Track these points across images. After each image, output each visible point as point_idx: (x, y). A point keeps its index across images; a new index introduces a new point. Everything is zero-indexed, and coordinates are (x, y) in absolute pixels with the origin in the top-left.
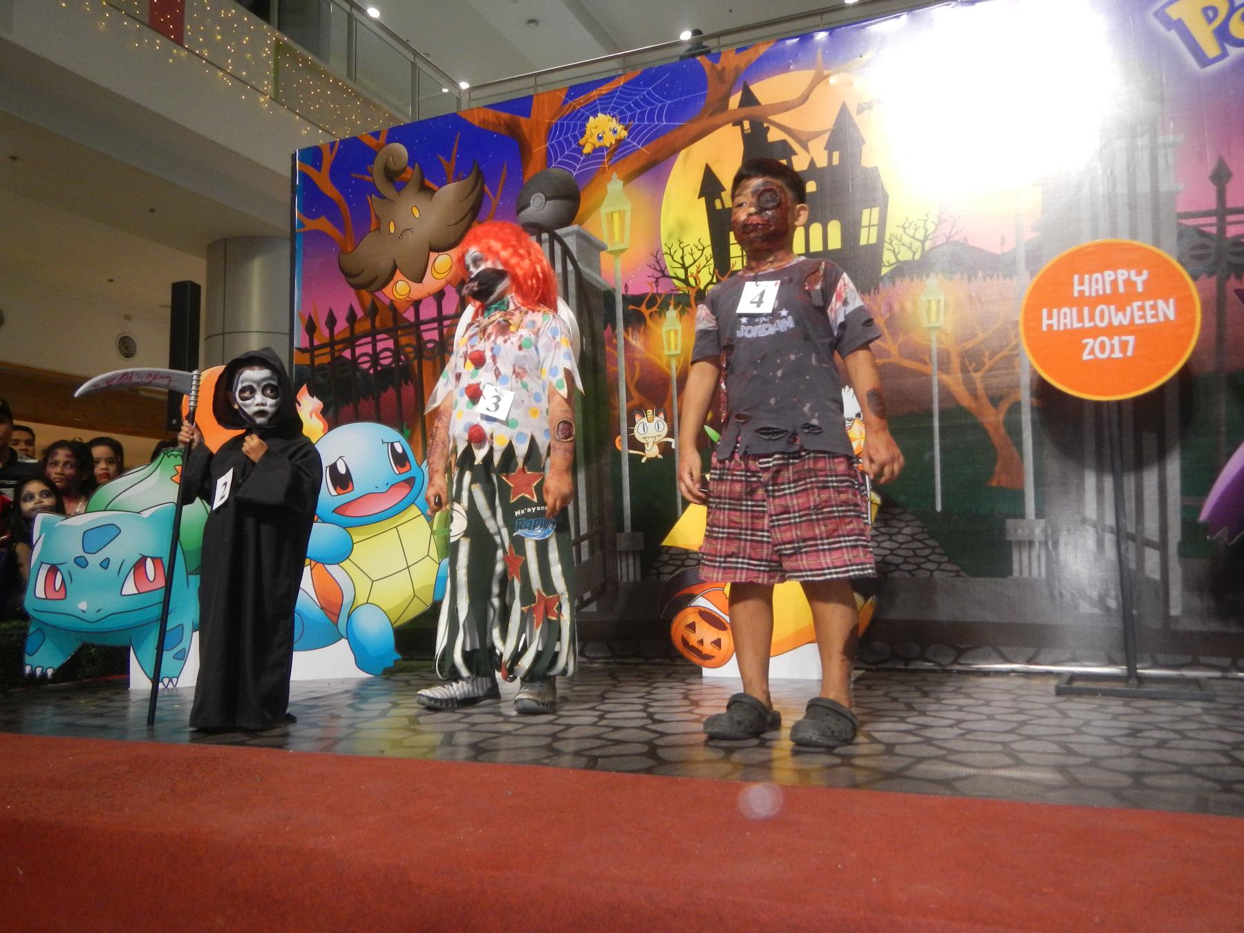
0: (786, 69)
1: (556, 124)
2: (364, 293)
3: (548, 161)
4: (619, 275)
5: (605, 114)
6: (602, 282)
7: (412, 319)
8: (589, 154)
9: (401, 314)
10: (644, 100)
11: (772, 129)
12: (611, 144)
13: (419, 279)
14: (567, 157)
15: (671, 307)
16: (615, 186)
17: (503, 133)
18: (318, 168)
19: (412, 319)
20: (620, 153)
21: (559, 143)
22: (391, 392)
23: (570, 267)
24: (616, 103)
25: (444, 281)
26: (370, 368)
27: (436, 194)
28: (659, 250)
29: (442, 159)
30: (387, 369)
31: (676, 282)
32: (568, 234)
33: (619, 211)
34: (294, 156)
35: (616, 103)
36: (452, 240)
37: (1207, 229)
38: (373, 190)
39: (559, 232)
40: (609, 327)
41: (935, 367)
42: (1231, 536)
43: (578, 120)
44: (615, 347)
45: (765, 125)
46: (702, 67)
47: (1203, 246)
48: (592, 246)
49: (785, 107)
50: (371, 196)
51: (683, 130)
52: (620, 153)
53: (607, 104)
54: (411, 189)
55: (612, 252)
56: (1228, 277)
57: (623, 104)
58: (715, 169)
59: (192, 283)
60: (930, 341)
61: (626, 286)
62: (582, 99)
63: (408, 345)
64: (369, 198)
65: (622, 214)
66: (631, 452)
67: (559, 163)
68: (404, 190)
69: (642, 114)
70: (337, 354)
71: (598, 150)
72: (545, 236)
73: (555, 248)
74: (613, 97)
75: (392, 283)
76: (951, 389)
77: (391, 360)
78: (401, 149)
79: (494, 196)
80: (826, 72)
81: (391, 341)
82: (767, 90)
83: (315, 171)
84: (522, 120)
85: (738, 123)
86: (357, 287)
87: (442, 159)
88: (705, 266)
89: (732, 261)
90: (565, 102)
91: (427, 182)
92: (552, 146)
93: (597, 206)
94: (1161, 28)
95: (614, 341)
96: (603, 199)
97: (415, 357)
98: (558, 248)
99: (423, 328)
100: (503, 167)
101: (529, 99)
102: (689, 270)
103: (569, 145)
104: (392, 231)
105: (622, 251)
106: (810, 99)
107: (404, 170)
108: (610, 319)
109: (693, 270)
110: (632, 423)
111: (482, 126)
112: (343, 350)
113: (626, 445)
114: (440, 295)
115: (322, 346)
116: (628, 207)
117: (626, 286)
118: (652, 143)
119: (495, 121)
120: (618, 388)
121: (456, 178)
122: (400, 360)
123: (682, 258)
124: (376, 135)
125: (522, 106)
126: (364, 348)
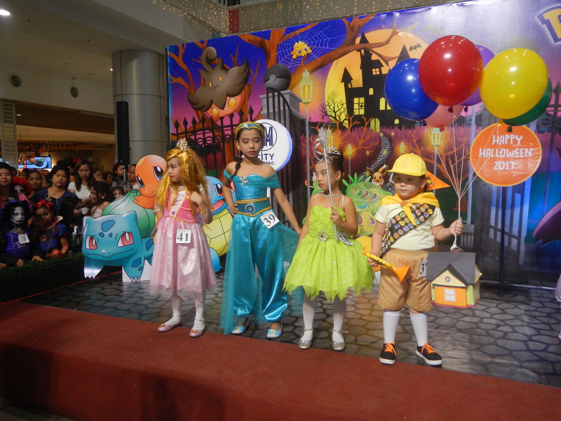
0: (381, 28)
1: (281, 44)
2: (199, 112)
3: (277, 60)
4: (307, 113)
5: (302, 41)
6: (300, 116)
7: (220, 125)
8: (295, 59)
9: (215, 123)
10: (319, 36)
11: (373, 54)
12: (304, 55)
13: (223, 108)
14: (285, 59)
15: (329, 128)
16: (306, 74)
17: (258, 46)
18: (177, 55)
19: (220, 125)
20: (308, 60)
21: (282, 53)
22: (212, 155)
23: (287, 108)
24: (307, 37)
25: (233, 109)
26: (202, 144)
27: (229, 71)
28: (324, 104)
29: (232, 56)
30: (210, 145)
31: (331, 117)
32: (286, 94)
33: (308, 85)
34: (166, 49)
35: (307, 37)
36: (237, 92)
37: (550, 112)
38: (201, 66)
39: (282, 92)
40: (303, 134)
41: (436, 161)
42: (544, 243)
43: (290, 43)
44: (305, 143)
45: (371, 52)
46: (344, 24)
47: (547, 120)
48: (296, 100)
49: (380, 45)
50: (201, 70)
51: (335, 51)
52: (308, 60)
53: (303, 37)
54: (218, 69)
55: (304, 103)
56: (556, 133)
57: (310, 38)
58: (348, 70)
59: (125, 102)
60: (434, 150)
61: (310, 118)
62: (292, 34)
63: (218, 136)
64: (200, 71)
65: (309, 87)
66: (311, 187)
67: (283, 62)
68: (215, 68)
69: (318, 43)
70: (188, 137)
71: (299, 57)
72: (276, 94)
73: (281, 99)
74: (306, 34)
75: (211, 108)
76: (442, 171)
77: (211, 141)
78: (213, 49)
79: (254, 74)
80: (397, 31)
81: (211, 133)
82: (373, 37)
83: (177, 57)
84: (266, 41)
85: (359, 50)
86: (196, 109)
87: (232, 56)
88: (343, 112)
89: (355, 111)
90: (285, 35)
91: (225, 66)
92: (279, 54)
93: (299, 82)
94: (540, 23)
95: (305, 141)
96: (301, 79)
97: (221, 141)
98: (281, 99)
99: (224, 129)
100: (258, 62)
101: (270, 31)
102: (337, 113)
103: (287, 54)
104: (210, 86)
105: (309, 103)
106: (390, 42)
107: (215, 59)
108: (304, 132)
109: (338, 113)
110: (312, 175)
111: (248, 42)
112: (191, 136)
113: (309, 184)
114: (231, 116)
115: (181, 133)
116: (311, 84)
117: (310, 118)
118: (322, 56)
119: (255, 41)
120: (306, 161)
121: (238, 65)
122: (216, 142)
123: (334, 108)
124: (202, 42)
125: (266, 35)
126: (200, 136)
